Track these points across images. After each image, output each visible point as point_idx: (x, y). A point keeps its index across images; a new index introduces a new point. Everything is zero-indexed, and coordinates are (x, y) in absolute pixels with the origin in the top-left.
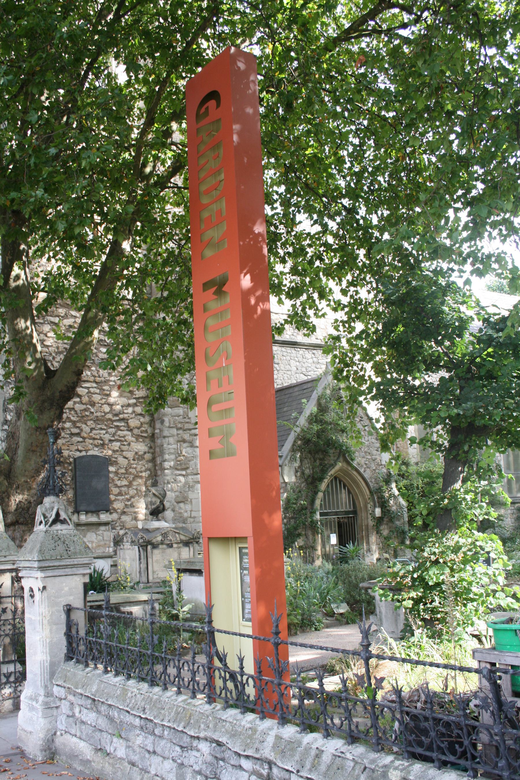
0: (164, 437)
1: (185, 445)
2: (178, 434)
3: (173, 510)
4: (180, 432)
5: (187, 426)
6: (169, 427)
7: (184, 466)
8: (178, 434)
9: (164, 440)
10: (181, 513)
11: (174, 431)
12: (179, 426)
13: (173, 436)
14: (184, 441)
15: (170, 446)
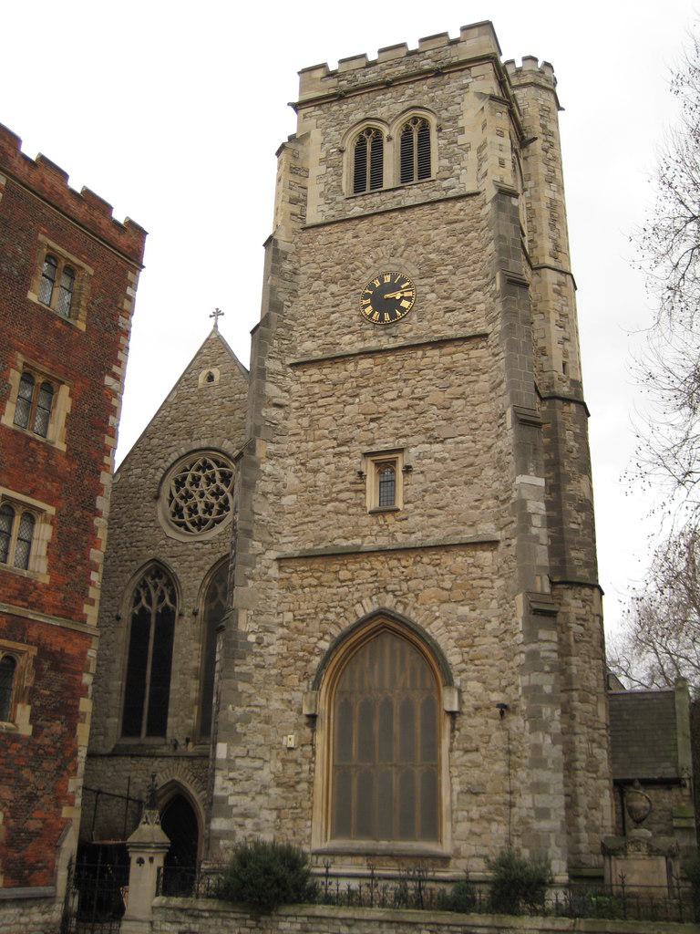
0: (575, 734)
1: (595, 745)
2: (588, 732)
3: (586, 817)
4: (590, 730)
5: (596, 725)
6: (580, 723)
7: (595, 769)
8: (588, 732)
9: (574, 738)
10: (593, 821)
11: (585, 729)
12: (589, 723)
13: (583, 734)
14: (593, 741)
15: (582, 745)
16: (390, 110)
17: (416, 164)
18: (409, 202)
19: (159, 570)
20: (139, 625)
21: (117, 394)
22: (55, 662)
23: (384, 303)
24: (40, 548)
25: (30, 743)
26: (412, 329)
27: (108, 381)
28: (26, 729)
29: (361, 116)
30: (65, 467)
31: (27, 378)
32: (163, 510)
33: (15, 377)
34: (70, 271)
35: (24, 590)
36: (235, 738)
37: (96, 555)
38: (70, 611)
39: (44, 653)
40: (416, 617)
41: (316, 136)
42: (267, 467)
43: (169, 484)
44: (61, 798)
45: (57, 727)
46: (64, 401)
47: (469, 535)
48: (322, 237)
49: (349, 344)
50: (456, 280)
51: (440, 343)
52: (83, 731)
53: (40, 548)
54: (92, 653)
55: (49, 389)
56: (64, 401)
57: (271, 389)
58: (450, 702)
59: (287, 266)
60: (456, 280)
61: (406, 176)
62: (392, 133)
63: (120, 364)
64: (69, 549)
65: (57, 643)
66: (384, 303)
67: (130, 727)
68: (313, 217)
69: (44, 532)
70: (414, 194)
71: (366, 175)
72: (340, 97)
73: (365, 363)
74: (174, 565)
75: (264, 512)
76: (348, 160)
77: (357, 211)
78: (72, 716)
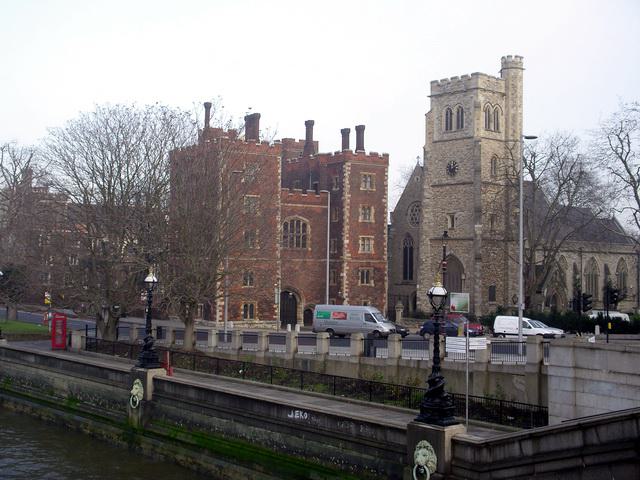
16: (454, 102)
17: (460, 125)
18: (458, 137)
19: (408, 235)
20: (405, 250)
21: (386, 203)
22: (378, 270)
23: (452, 171)
24: (372, 246)
25: (374, 288)
26: (459, 178)
27: (384, 200)
28: (373, 285)
29: (446, 103)
30: (374, 226)
31: (364, 208)
32: (409, 218)
33: (360, 210)
34: (370, 176)
35: (369, 256)
36: (421, 284)
37: (385, 244)
38: (380, 258)
39: (375, 269)
40: (458, 256)
41: (435, 108)
42: (425, 216)
43: (410, 211)
44: (383, 298)
45: (380, 284)
46: (373, 211)
47: (468, 236)
48: (439, 145)
49: (445, 181)
50: (468, 165)
51: (464, 184)
52: (386, 284)
53: (372, 246)
54: (387, 267)
55: (369, 208)
56: (373, 211)
57: (426, 194)
58: (463, 277)
59: (428, 156)
60: (468, 165)
61: (458, 127)
62: (454, 111)
63: (386, 195)
64: (378, 244)
65: (378, 266)
66: (452, 171)
67: (405, 277)
68: (436, 139)
69: (372, 242)
70: (459, 135)
71: (449, 126)
72: (440, 96)
73: (448, 187)
74: (412, 235)
75: (426, 228)
76: (444, 118)
77: (445, 138)
78: (383, 281)
